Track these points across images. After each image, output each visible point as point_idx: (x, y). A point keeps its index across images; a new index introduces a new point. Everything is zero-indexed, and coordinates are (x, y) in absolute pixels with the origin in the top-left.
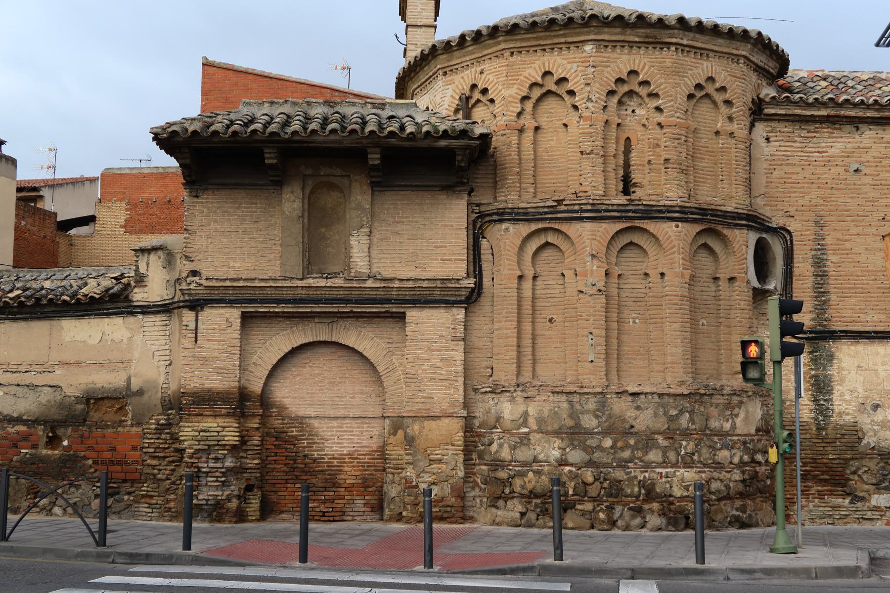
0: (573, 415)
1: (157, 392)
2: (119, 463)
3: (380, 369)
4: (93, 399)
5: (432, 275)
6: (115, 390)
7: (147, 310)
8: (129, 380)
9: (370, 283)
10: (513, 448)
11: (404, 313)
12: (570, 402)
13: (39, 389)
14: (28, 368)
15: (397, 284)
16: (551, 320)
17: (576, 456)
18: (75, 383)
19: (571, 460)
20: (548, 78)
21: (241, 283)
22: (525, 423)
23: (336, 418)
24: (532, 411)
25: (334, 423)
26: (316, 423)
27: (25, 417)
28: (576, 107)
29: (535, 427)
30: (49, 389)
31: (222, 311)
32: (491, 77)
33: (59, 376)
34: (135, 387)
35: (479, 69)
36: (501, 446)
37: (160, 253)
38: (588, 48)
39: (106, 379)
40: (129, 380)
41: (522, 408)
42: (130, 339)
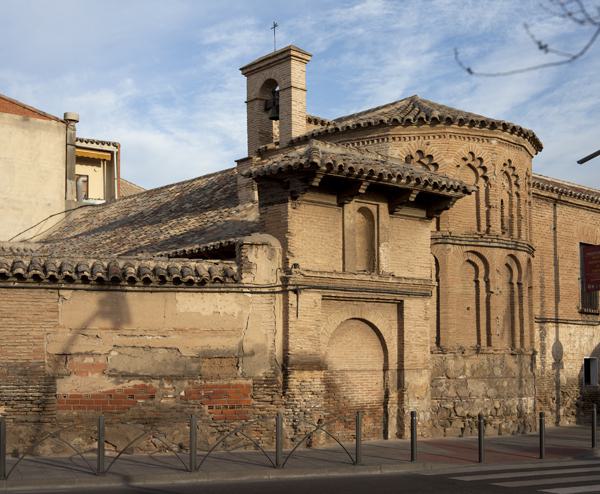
0: (491, 368)
1: (265, 353)
2: (232, 407)
3: (385, 338)
4: (206, 355)
5: (416, 276)
6: (229, 352)
7: (255, 290)
8: (241, 343)
9: (391, 280)
10: (456, 388)
11: (402, 301)
12: (488, 360)
13: (154, 350)
14: (142, 333)
15: (404, 281)
16: (468, 309)
17: (491, 392)
18: (190, 346)
19: (488, 394)
20: (479, 162)
21: (326, 275)
22: (463, 374)
23: (360, 371)
24: (468, 365)
25: (359, 375)
26: (349, 374)
27: (141, 374)
28: (486, 178)
29: (469, 375)
30: (166, 351)
31: (311, 295)
32: (435, 149)
33: (174, 340)
34: (247, 347)
35: (425, 141)
36: (448, 388)
37: (265, 247)
38: (494, 142)
39: (217, 343)
40: (241, 343)
41: (462, 364)
42: (241, 313)
